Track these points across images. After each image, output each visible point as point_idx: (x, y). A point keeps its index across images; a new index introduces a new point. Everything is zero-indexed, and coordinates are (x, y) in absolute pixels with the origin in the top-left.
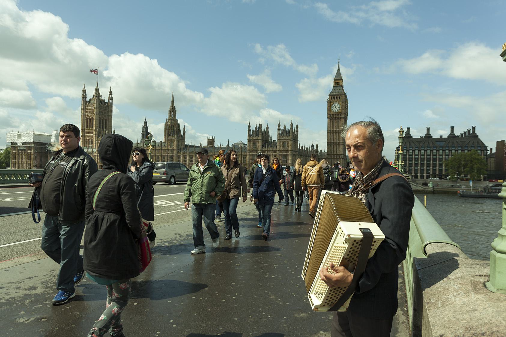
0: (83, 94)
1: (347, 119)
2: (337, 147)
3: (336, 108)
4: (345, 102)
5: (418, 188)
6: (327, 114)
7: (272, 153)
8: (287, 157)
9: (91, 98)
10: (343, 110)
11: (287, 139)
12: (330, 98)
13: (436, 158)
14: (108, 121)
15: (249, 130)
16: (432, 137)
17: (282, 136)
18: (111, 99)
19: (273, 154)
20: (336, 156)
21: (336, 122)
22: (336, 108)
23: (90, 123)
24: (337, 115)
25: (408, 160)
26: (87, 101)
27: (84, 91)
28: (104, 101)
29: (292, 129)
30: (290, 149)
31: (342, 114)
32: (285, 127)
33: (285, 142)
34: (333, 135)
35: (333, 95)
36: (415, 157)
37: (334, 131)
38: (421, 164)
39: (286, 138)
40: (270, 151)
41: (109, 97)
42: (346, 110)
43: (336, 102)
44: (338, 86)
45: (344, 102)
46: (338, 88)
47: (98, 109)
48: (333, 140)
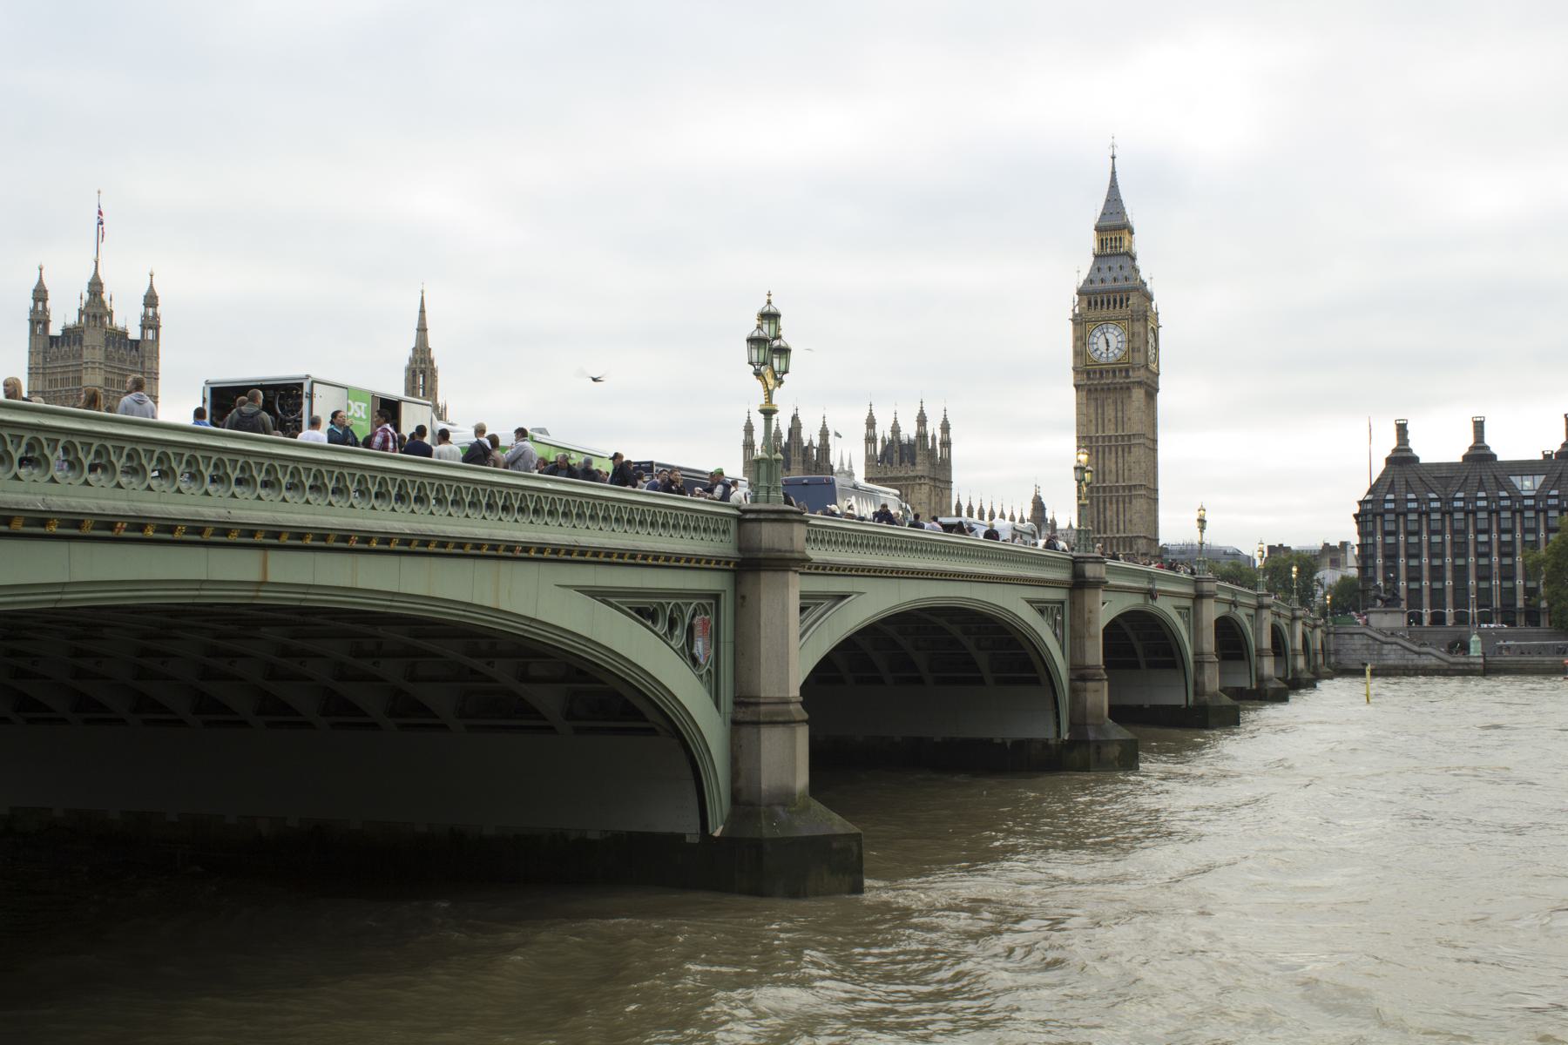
1: (1157, 390)
2: (1121, 505)
3: (1110, 343)
4: (1146, 320)
5: (1426, 662)
10: (1139, 351)
11: (906, 479)
12: (1085, 305)
13: (1512, 543)
16: (1493, 457)
17: (885, 467)
18: (151, 323)
20: (1118, 545)
21: (1110, 401)
24: (1114, 372)
25: (1402, 552)
26: (52, 338)
27: (40, 294)
28: (124, 334)
29: (922, 436)
32: (896, 429)
34: (1100, 456)
35: (1095, 293)
36: (1429, 540)
37: (1104, 442)
38: (1455, 566)
41: (145, 316)
42: (1151, 352)
43: (1107, 321)
45: (1138, 320)
46: (1115, 263)
48: (1101, 477)
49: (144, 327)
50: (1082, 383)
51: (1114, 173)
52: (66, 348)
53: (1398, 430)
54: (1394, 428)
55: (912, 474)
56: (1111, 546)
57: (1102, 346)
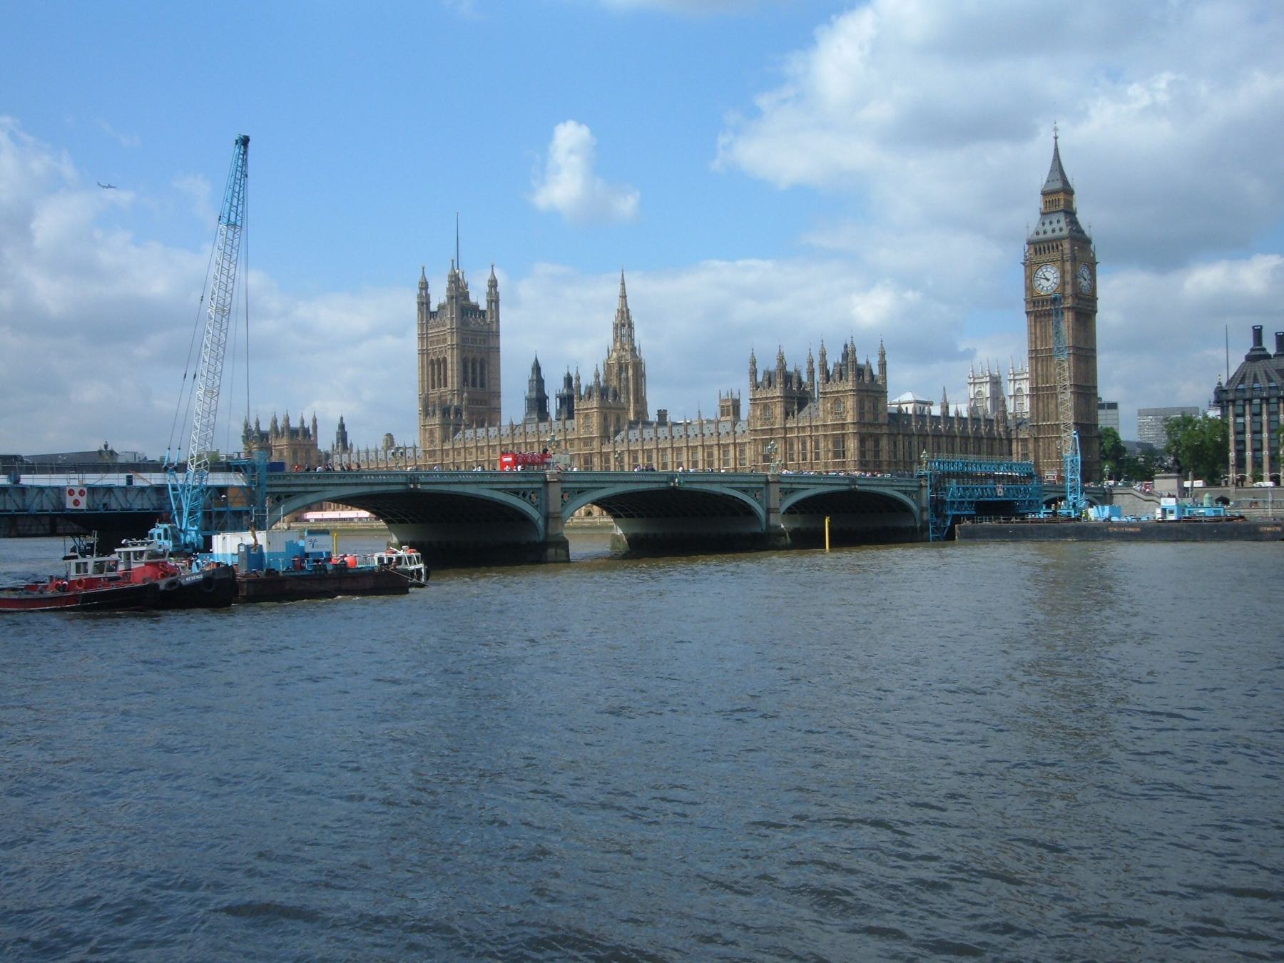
0: (421, 294)
1: (1096, 312)
6: (1025, 300)
7: (809, 434)
8: (843, 441)
9: (442, 302)
12: (1032, 251)
14: (489, 364)
15: (754, 373)
18: (494, 300)
19: (811, 436)
22: (1049, 279)
23: (439, 374)
26: (433, 313)
30: (849, 420)
31: (1064, 297)
33: (837, 399)
37: (1046, 353)
39: (840, 389)
40: (804, 428)
41: (489, 294)
43: (1046, 263)
44: (1053, 212)
47: (457, 332)
49: (490, 302)
50: (1031, 310)
51: (1056, 150)
52: (438, 319)
53: (1254, 334)
54: (1251, 333)
55: (847, 388)
56: (1053, 430)
57: (1043, 282)
